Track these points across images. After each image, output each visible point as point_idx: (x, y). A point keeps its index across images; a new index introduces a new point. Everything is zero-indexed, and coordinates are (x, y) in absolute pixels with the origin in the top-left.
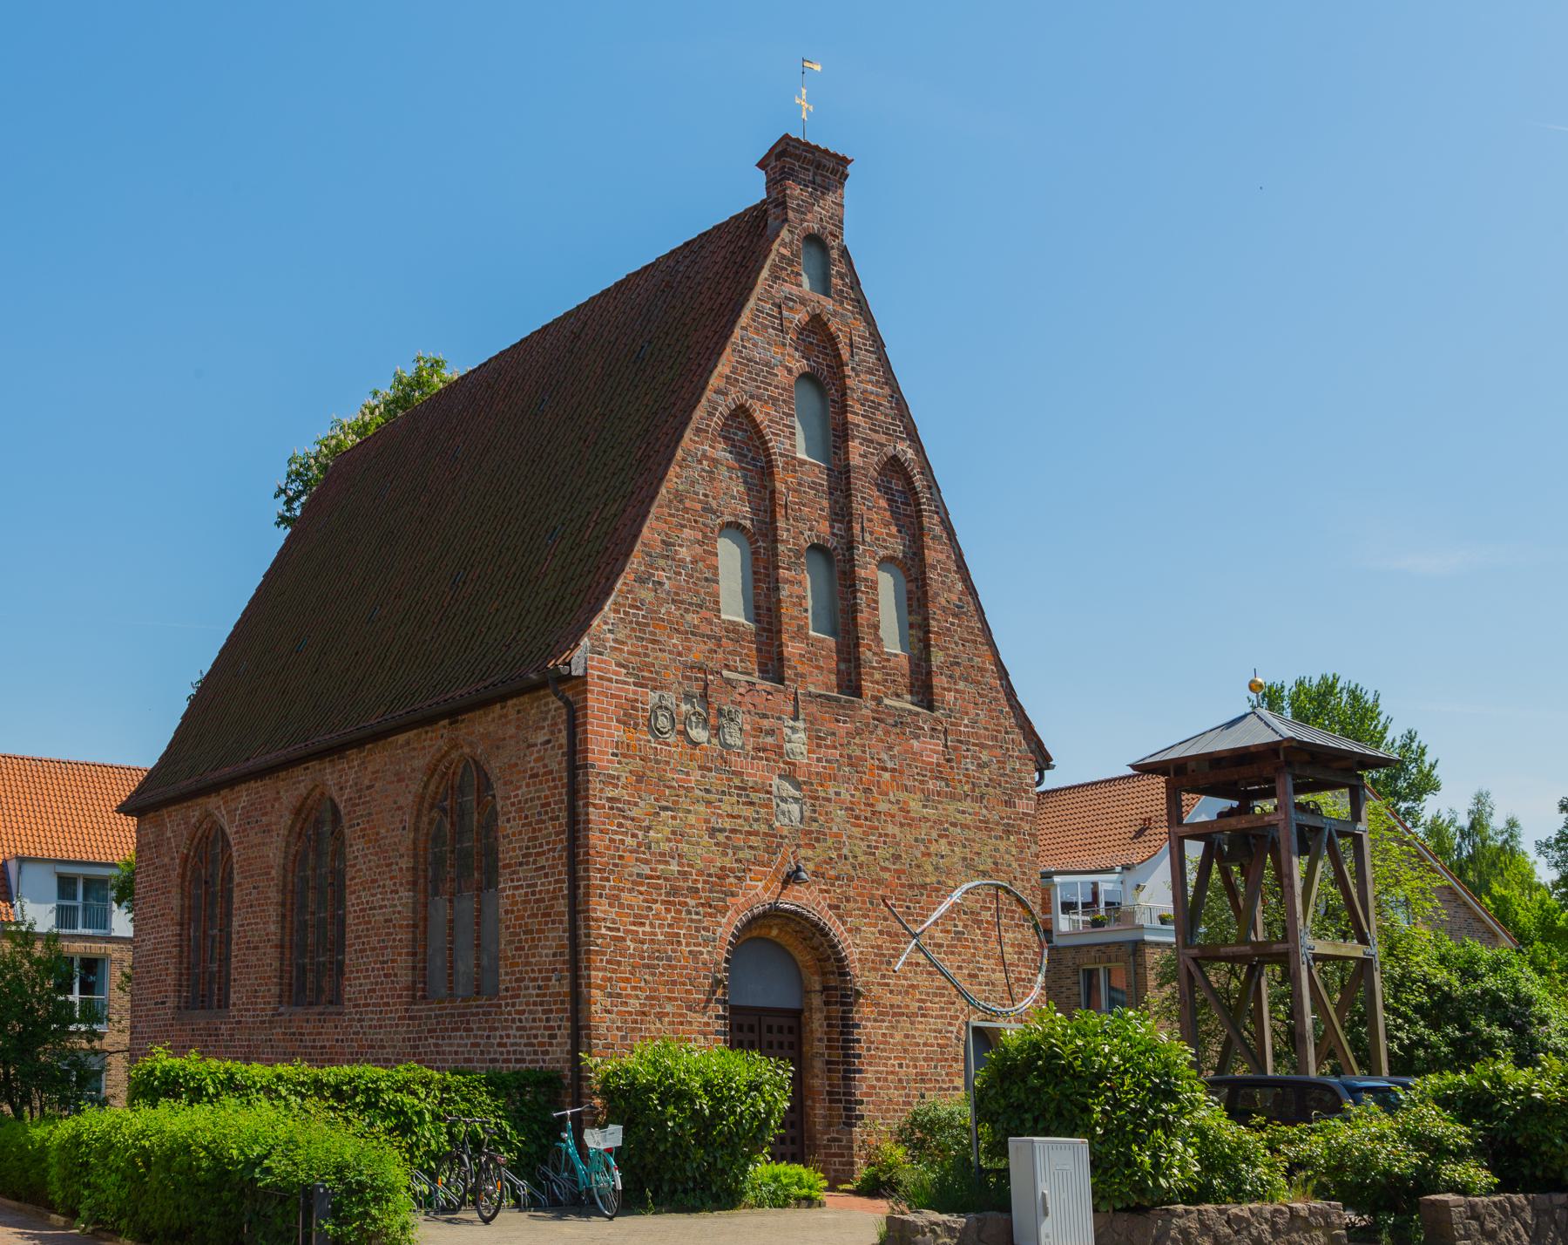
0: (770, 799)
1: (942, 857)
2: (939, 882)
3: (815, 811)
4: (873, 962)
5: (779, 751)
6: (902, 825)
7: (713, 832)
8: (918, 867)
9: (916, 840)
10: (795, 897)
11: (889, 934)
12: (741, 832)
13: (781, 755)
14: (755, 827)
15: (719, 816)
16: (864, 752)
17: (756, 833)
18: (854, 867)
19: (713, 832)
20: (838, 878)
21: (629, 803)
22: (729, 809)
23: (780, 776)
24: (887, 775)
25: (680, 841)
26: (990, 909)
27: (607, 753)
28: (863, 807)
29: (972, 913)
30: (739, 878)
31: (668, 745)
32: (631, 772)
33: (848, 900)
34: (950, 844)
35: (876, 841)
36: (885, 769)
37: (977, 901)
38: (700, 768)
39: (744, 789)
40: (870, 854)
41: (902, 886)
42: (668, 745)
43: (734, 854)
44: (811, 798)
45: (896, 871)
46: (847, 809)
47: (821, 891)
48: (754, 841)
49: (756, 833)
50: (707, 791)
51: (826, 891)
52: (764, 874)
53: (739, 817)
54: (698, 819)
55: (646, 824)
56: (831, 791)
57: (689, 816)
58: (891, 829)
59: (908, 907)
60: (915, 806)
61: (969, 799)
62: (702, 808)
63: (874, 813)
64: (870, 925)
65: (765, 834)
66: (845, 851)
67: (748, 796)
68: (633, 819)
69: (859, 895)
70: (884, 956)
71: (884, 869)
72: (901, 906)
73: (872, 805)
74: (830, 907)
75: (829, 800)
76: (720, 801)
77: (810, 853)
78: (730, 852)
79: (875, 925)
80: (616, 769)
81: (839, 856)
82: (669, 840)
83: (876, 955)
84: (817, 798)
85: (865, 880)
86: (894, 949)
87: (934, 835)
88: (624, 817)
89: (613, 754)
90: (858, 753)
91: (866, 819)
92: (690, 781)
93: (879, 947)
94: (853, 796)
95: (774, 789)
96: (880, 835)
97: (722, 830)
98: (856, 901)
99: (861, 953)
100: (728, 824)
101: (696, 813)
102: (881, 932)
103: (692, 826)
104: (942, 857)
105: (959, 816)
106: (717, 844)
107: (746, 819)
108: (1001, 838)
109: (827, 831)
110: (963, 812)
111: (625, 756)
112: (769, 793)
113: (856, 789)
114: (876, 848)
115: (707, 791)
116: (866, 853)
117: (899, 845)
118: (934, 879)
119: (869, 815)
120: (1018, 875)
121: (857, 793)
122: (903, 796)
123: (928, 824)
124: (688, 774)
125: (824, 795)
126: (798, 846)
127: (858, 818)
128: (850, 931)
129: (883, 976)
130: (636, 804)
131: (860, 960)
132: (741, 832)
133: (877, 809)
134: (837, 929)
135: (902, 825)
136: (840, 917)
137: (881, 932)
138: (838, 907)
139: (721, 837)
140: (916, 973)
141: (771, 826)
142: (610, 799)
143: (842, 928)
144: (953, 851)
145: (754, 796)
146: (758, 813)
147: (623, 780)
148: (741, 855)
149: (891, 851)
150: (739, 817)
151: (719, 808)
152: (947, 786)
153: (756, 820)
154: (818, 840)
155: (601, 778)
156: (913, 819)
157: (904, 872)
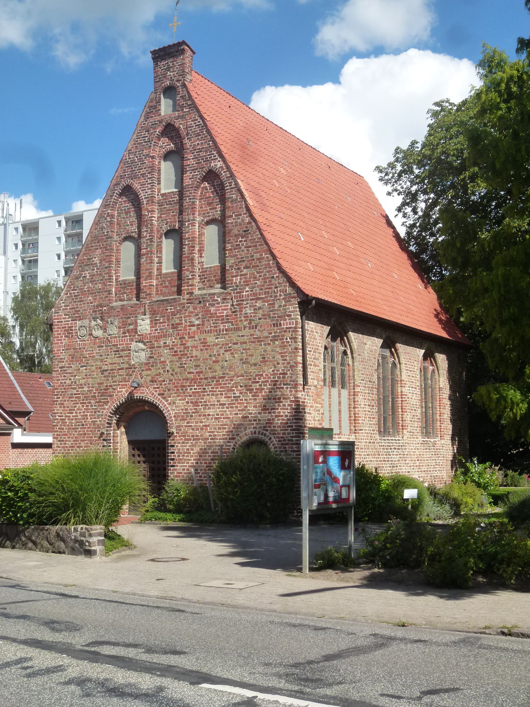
0: (130, 353)
1: (226, 361)
2: (224, 374)
3: (152, 354)
4: (182, 416)
5: (135, 331)
6: (202, 350)
7: (103, 372)
8: (210, 368)
9: (210, 356)
10: (141, 393)
11: (192, 403)
12: (115, 370)
13: (136, 332)
14: (122, 366)
15: (106, 365)
16: (181, 320)
17: (122, 369)
18: (172, 375)
19: (103, 372)
20: (164, 381)
21: (68, 367)
22: (110, 361)
23: (136, 342)
24: (194, 328)
25: (89, 378)
26: (258, 382)
27: (60, 350)
28: (179, 346)
29: (246, 386)
30: (114, 389)
31: (84, 341)
32: (69, 355)
33: (169, 390)
34: (232, 354)
35: (186, 361)
36: (194, 326)
37: (250, 379)
38: (98, 347)
39: (118, 351)
40: (182, 367)
41: (201, 379)
42: (84, 341)
43: (112, 379)
44: (150, 348)
45: (197, 373)
46: (170, 349)
47: (154, 388)
48: (121, 372)
49: (122, 369)
50: (101, 356)
51: (157, 388)
52: (126, 385)
53: (115, 363)
54: (97, 368)
55: (75, 374)
56: (162, 343)
57: (93, 367)
58: (195, 353)
59: (204, 389)
60: (211, 339)
61: (247, 329)
62: (98, 363)
63: (185, 348)
64: (180, 400)
65: (127, 368)
66: (168, 368)
67: (119, 354)
68: (70, 373)
69: (175, 387)
70: (189, 413)
71: (189, 373)
72: (200, 389)
73: (185, 344)
74: (159, 395)
75: (160, 347)
76: (107, 358)
77: (149, 372)
78: (110, 379)
79: (184, 399)
80: (63, 355)
81: (164, 371)
82: (84, 379)
83: (184, 413)
84: (154, 348)
85: (180, 380)
86: (195, 409)
87: (222, 351)
88: (66, 373)
89: (63, 350)
90: (178, 321)
91: (181, 351)
92: (93, 353)
93: (187, 409)
94: (173, 342)
95: (132, 348)
96: (188, 358)
97: (106, 370)
98: (173, 390)
99: (176, 413)
100: (110, 367)
101: (96, 365)
102: (187, 402)
103: (94, 371)
104: (226, 361)
105: (239, 338)
106: (104, 377)
107: (119, 363)
108: (269, 344)
109: (158, 361)
110: (243, 336)
111: (67, 349)
112: (130, 350)
113: (175, 339)
114: (185, 364)
115: (101, 356)
116: (179, 367)
117: (199, 360)
118: (221, 373)
119: (182, 349)
120: (281, 362)
121: (176, 341)
122: (202, 336)
123: (219, 346)
124: (93, 351)
125: (158, 345)
126: (143, 370)
127: (176, 352)
128: (170, 404)
129: (188, 423)
130: (71, 367)
131: (175, 417)
132: (115, 370)
133: (187, 345)
134: (163, 404)
135: (202, 350)
136: (164, 398)
137: (187, 402)
138: (163, 394)
139: (106, 373)
140: (208, 419)
141: (130, 365)
142: (60, 368)
143: (166, 403)
144: (234, 357)
145: (122, 353)
146: (124, 360)
147: (66, 359)
148: (115, 379)
149: (195, 363)
150: (115, 363)
151: (106, 361)
152: (233, 325)
153: (122, 363)
154: (152, 366)
155: (58, 360)
156: (209, 346)
157: (202, 372)
